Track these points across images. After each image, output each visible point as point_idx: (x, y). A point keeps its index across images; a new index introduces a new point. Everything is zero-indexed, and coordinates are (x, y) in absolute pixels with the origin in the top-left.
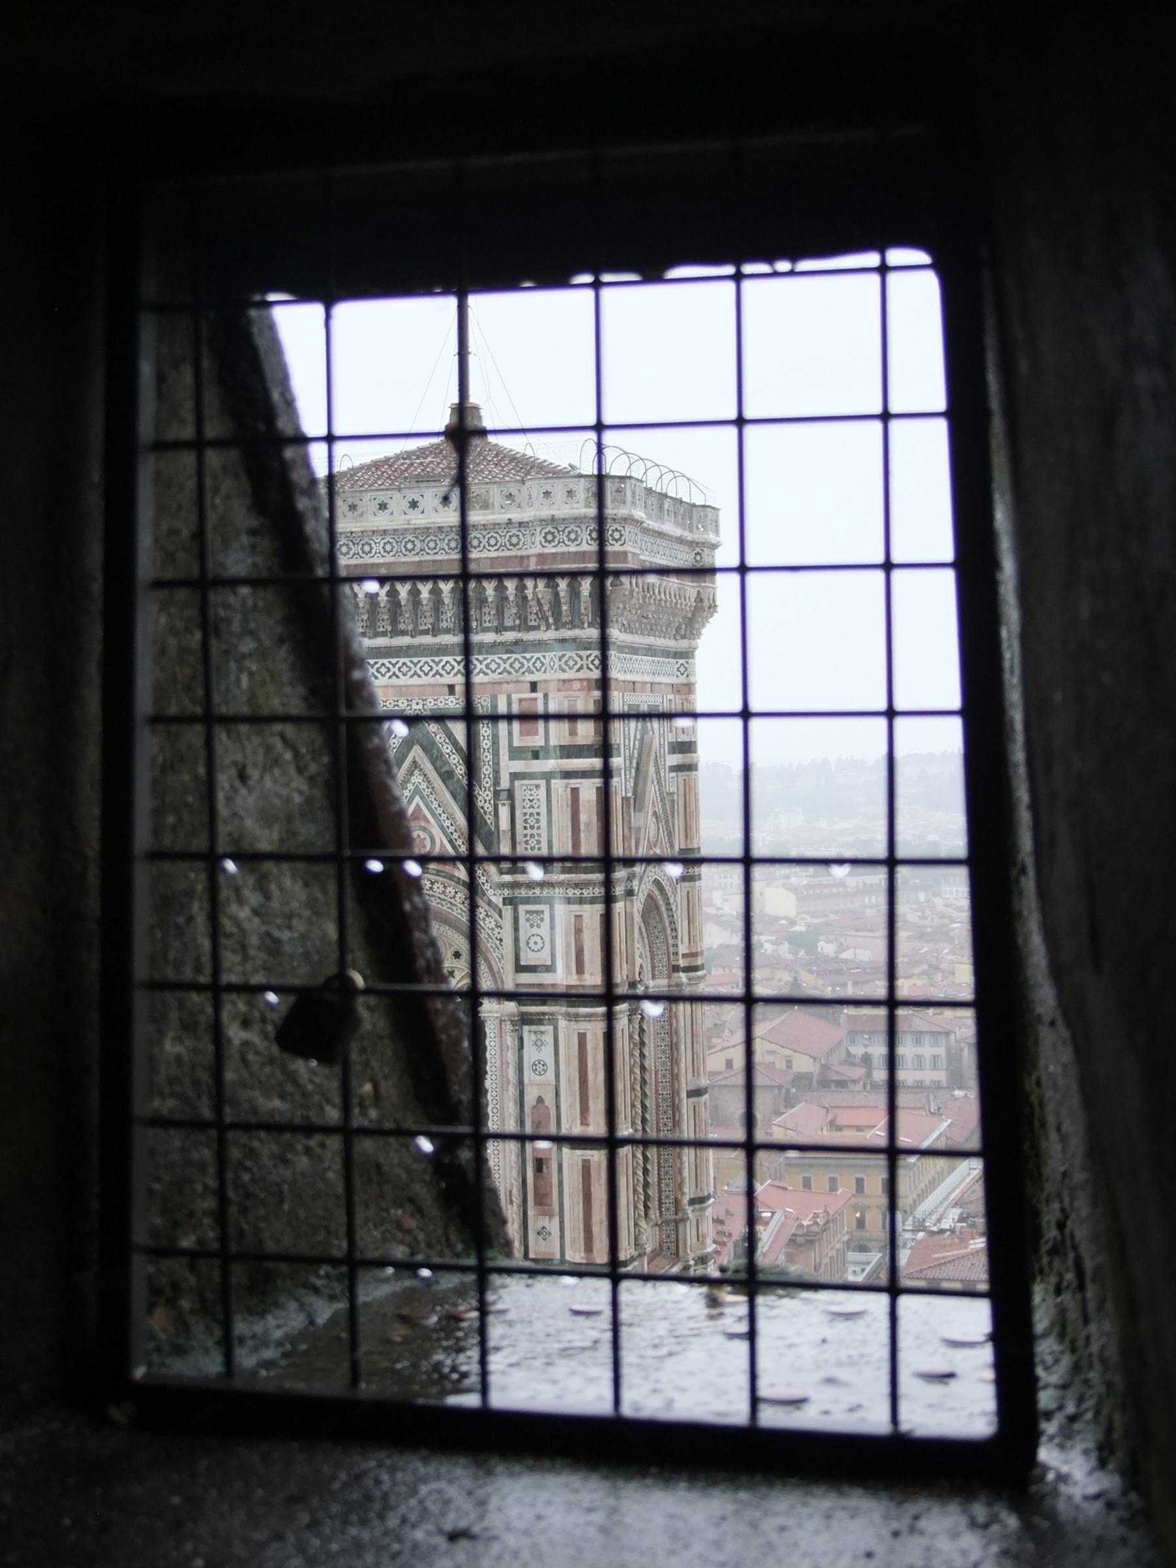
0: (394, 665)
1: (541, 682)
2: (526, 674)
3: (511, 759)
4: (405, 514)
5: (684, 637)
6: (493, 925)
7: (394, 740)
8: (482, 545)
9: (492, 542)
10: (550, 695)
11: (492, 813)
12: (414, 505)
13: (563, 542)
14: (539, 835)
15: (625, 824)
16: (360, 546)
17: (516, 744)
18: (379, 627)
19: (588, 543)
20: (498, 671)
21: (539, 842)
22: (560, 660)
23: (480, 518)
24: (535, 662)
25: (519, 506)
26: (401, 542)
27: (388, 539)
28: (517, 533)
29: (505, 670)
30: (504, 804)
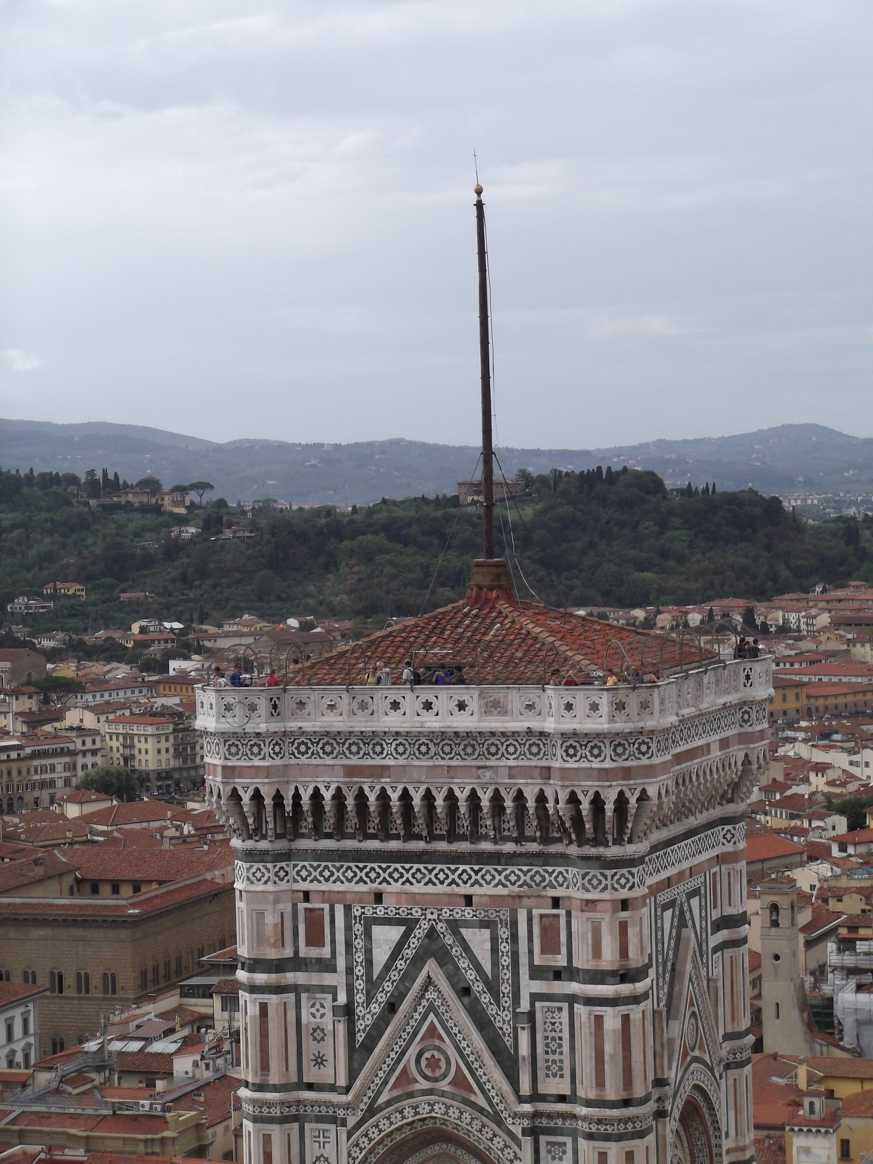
0: (408, 871)
1: (563, 898)
2: (548, 888)
3: (532, 978)
4: (418, 715)
5: (731, 801)
6: (511, 1156)
7: (407, 951)
8: (500, 753)
9: (511, 749)
10: (574, 913)
11: (511, 1035)
12: (428, 706)
13: (586, 757)
14: (561, 1061)
15: (657, 1037)
16: (371, 746)
17: (536, 962)
18: (392, 829)
19: (611, 759)
20: (519, 883)
21: (561, 1069)
22: (583, 879)
24: (557, 877)
25: (540, 714)
26: (414, 744)
27: (401, 740)
28: (537, 742)
29: (525, 883)
30: (523, 1028)
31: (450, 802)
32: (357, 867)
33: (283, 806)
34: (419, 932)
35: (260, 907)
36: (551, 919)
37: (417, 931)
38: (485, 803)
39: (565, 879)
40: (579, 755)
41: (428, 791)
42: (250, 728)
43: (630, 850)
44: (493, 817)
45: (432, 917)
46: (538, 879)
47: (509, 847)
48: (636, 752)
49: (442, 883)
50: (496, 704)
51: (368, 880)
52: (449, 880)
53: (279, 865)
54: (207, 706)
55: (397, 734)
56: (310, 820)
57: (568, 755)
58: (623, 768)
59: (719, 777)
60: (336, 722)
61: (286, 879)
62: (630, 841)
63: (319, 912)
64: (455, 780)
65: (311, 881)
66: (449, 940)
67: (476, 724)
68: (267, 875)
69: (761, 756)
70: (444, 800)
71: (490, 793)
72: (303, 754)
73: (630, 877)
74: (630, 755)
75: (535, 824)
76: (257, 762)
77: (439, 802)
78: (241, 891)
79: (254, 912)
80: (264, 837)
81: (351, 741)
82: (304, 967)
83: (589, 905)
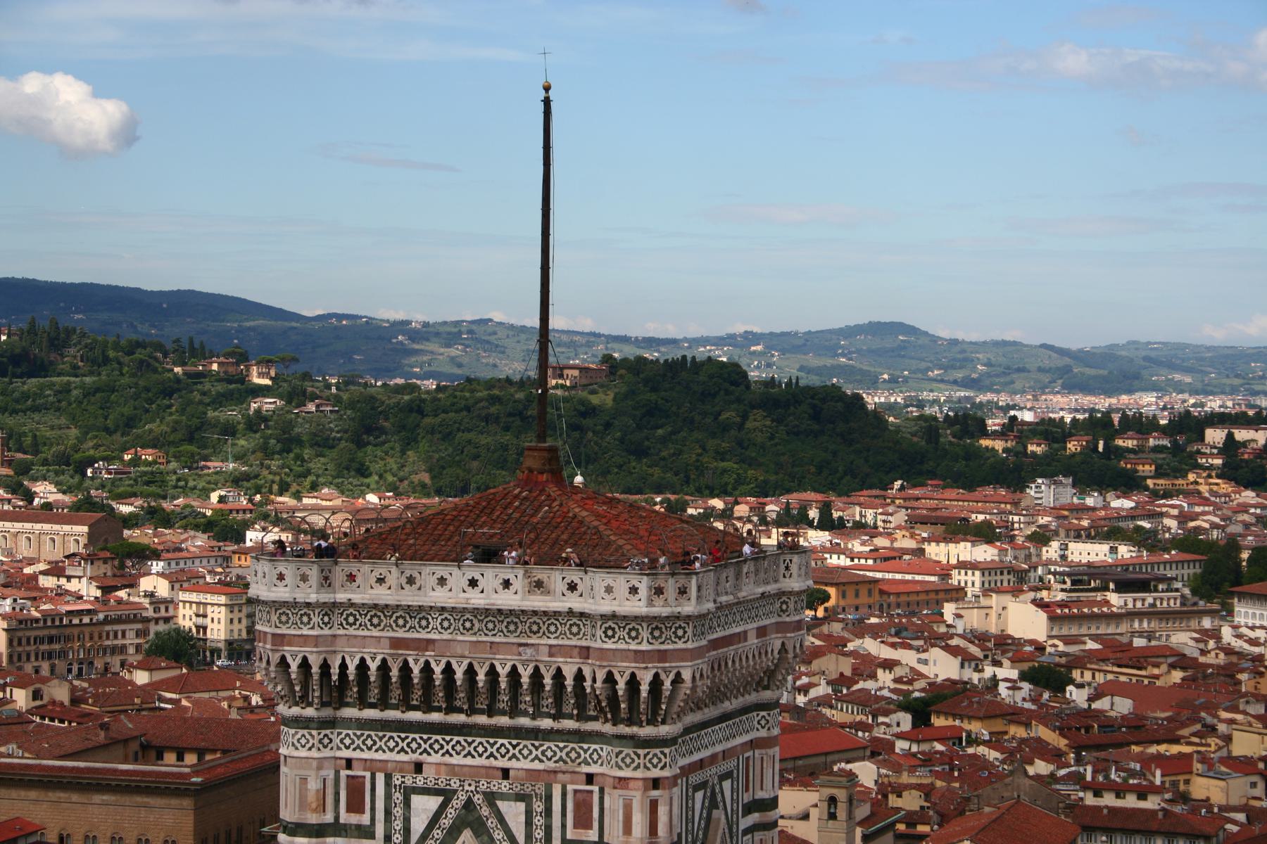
0: (448, 743)
1: (597, 774)
4: (464, 591)
5: (767, 688)
8: (541, 631)
9: (552, 629)
10: (607, 790)
12: (473, 583)
13: (624, 639)
17: (569, 836)
20: (554, 759)
22: (617, 757)
23: (541, 604)
24: (592, 754)
25: (581, 595)
27: (446, 615)
28: (578, 622)
29: (561, 759)
31: (490, 677)
32: (399, 737)
33: (330, 675)
34: (457, 803)
35: (303, 772)
36: (585, 794)
37: (454, 802)
38: (525, 680)
39: (600, 757)
40: (617, 636)
41: (471, 666)
42: (301, 597)
43: (664, 730)
44: (532, 693)
45: (470, 789)
46: (573, 755)
47: (546, 723)
48: (673, 636)
49: (480, 756)
50: (539, 584)
51: (409, 750)
52: (488, 753)
53: (324, 732)
54: (260, 574)
55: (443, 609)
56: (355, 690)
57: (606, 636)
58: (659, 651)
59: (755, 664)
60: (383, 595)
61: (330, 746)
62: (663, 722)
63: (361, 780)
64: (497, 657)
65: (354, 749)
66: (485, 811)
67: (519, 603)
68: (311, 742)
69: (798, 646)
70: (486, 675)
71: (530, 670)
72: (351, 625)
73: (662, 757)
74: (666, 639)
75: (572, 701)
76: (305, 632)
77: (481, 677)
78: (285, 757)
79: (298, 778)
80: (310, 704)
81: (398, 614)
82: (343, 833)
83: (622, 782)
